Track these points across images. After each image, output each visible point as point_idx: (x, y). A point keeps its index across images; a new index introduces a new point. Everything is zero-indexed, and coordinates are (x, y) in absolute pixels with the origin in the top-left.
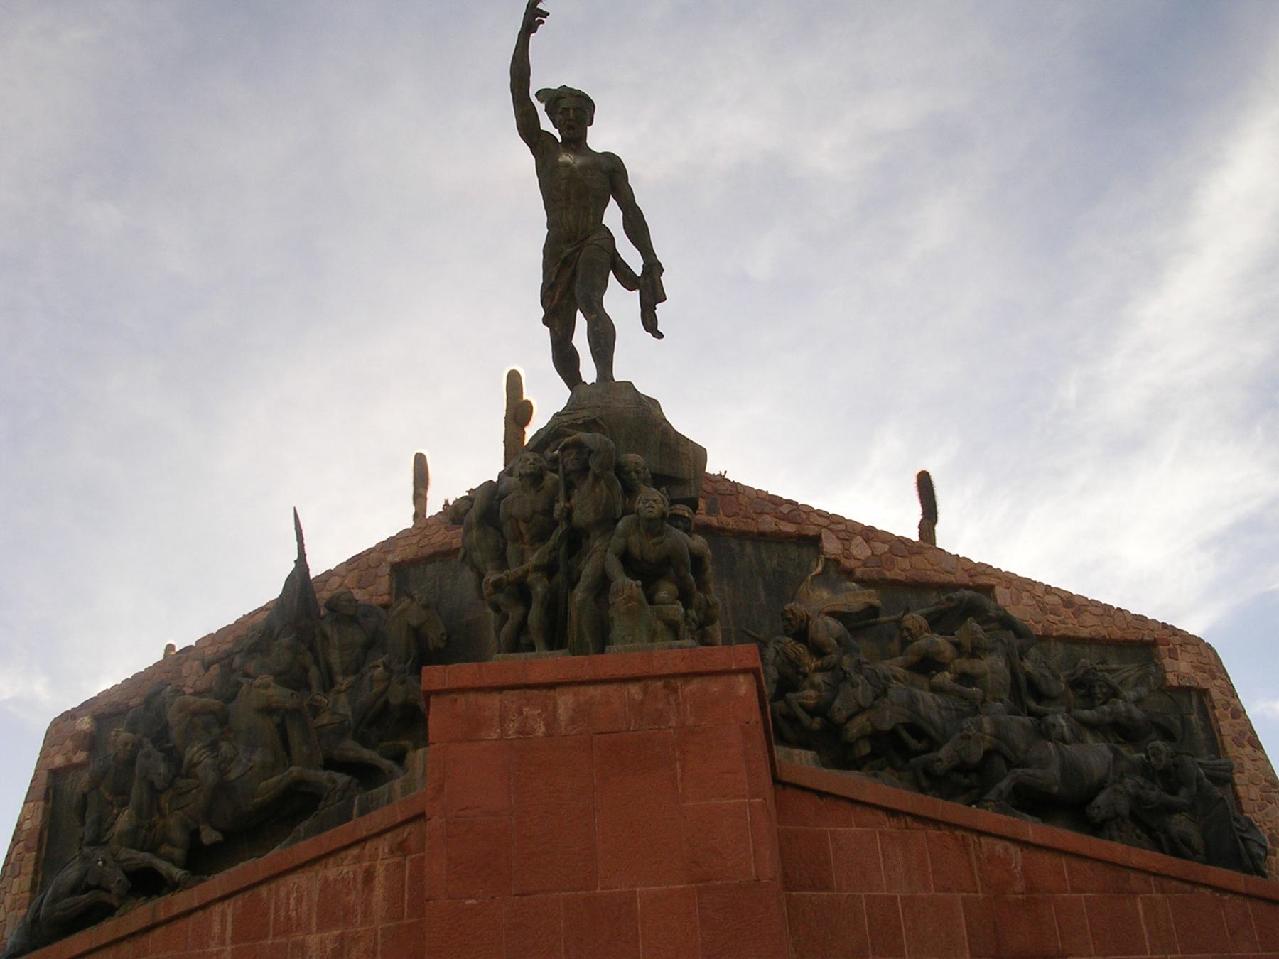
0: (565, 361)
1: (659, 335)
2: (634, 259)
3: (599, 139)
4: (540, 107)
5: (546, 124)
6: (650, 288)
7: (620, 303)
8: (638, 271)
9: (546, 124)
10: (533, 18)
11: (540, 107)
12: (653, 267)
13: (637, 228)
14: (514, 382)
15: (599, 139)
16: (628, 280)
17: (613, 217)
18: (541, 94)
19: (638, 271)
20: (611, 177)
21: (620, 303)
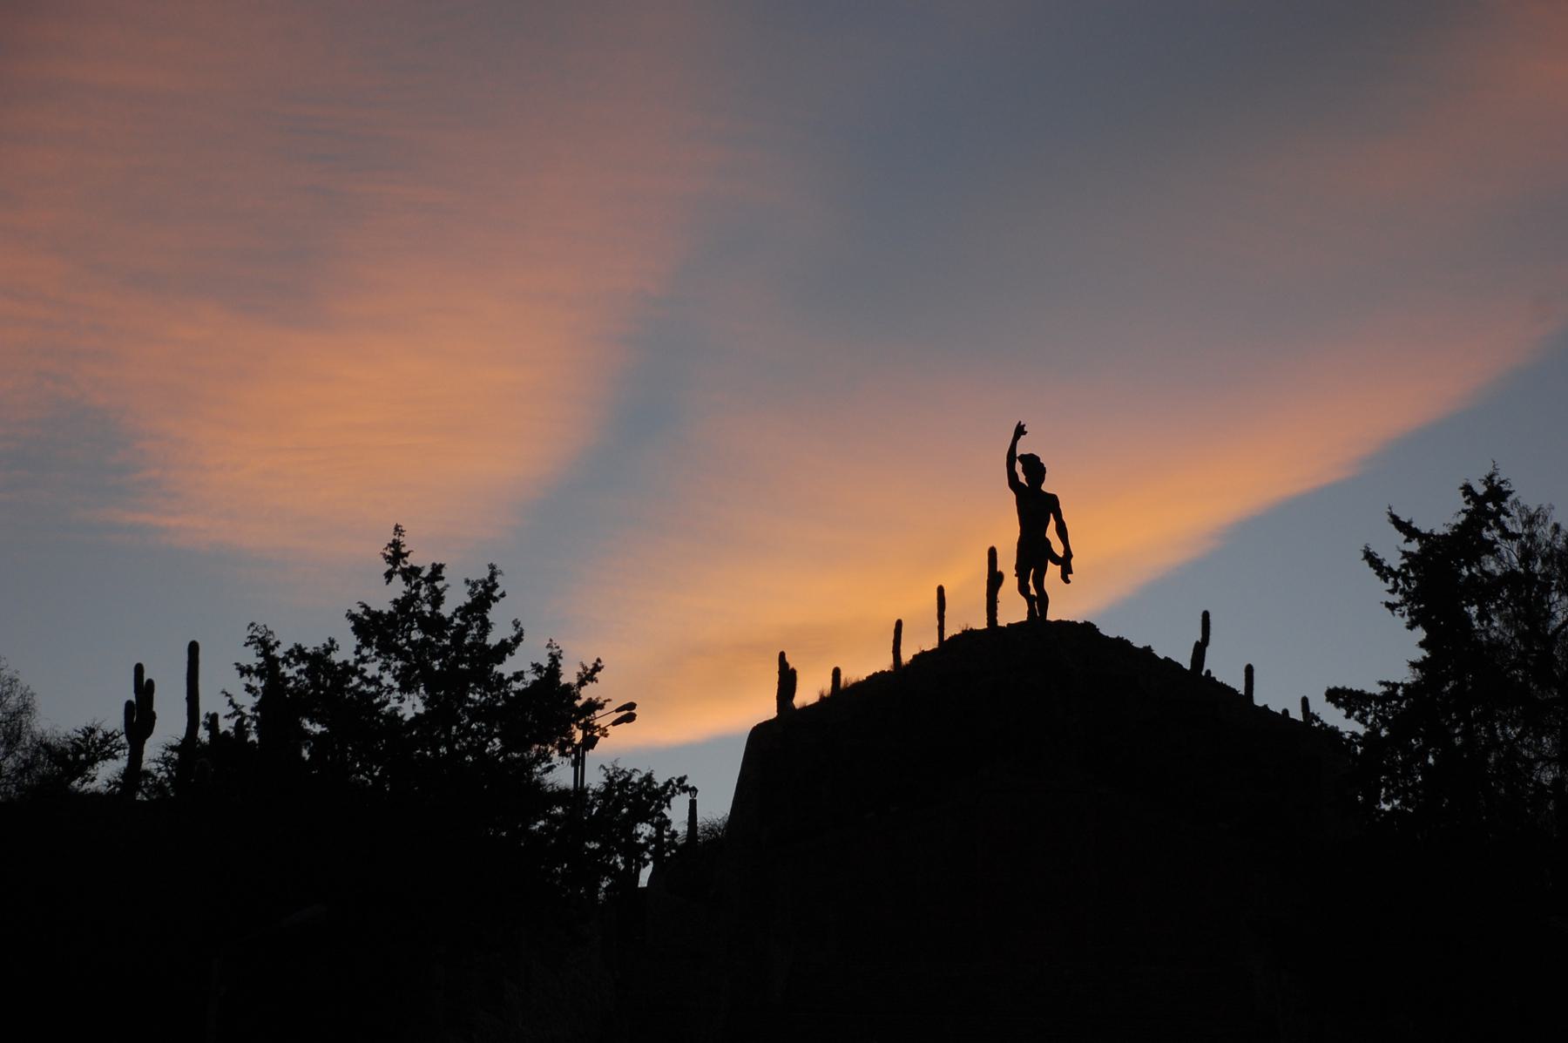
0: (1023, 589)
1: (1067, 581)
2: (1058, 548)
3: (1046, 487)
4: (1019, 467)
5: (1022, 478)
6: (1066, 571)
7: (1053, 571)
8: (1061, 554)
9: (1022, 478)
10: (1020, 431)
11: (1019, 467)
12: (1068, 554)
13: (1062, 531)
14: (992, 553)
15: (1046, 487)
16: (1056, 560)
17: (1051, 532)
18: (1023, 458)
19: (1061, 554)
20: (1052, 504)
21: (1053, 571)
